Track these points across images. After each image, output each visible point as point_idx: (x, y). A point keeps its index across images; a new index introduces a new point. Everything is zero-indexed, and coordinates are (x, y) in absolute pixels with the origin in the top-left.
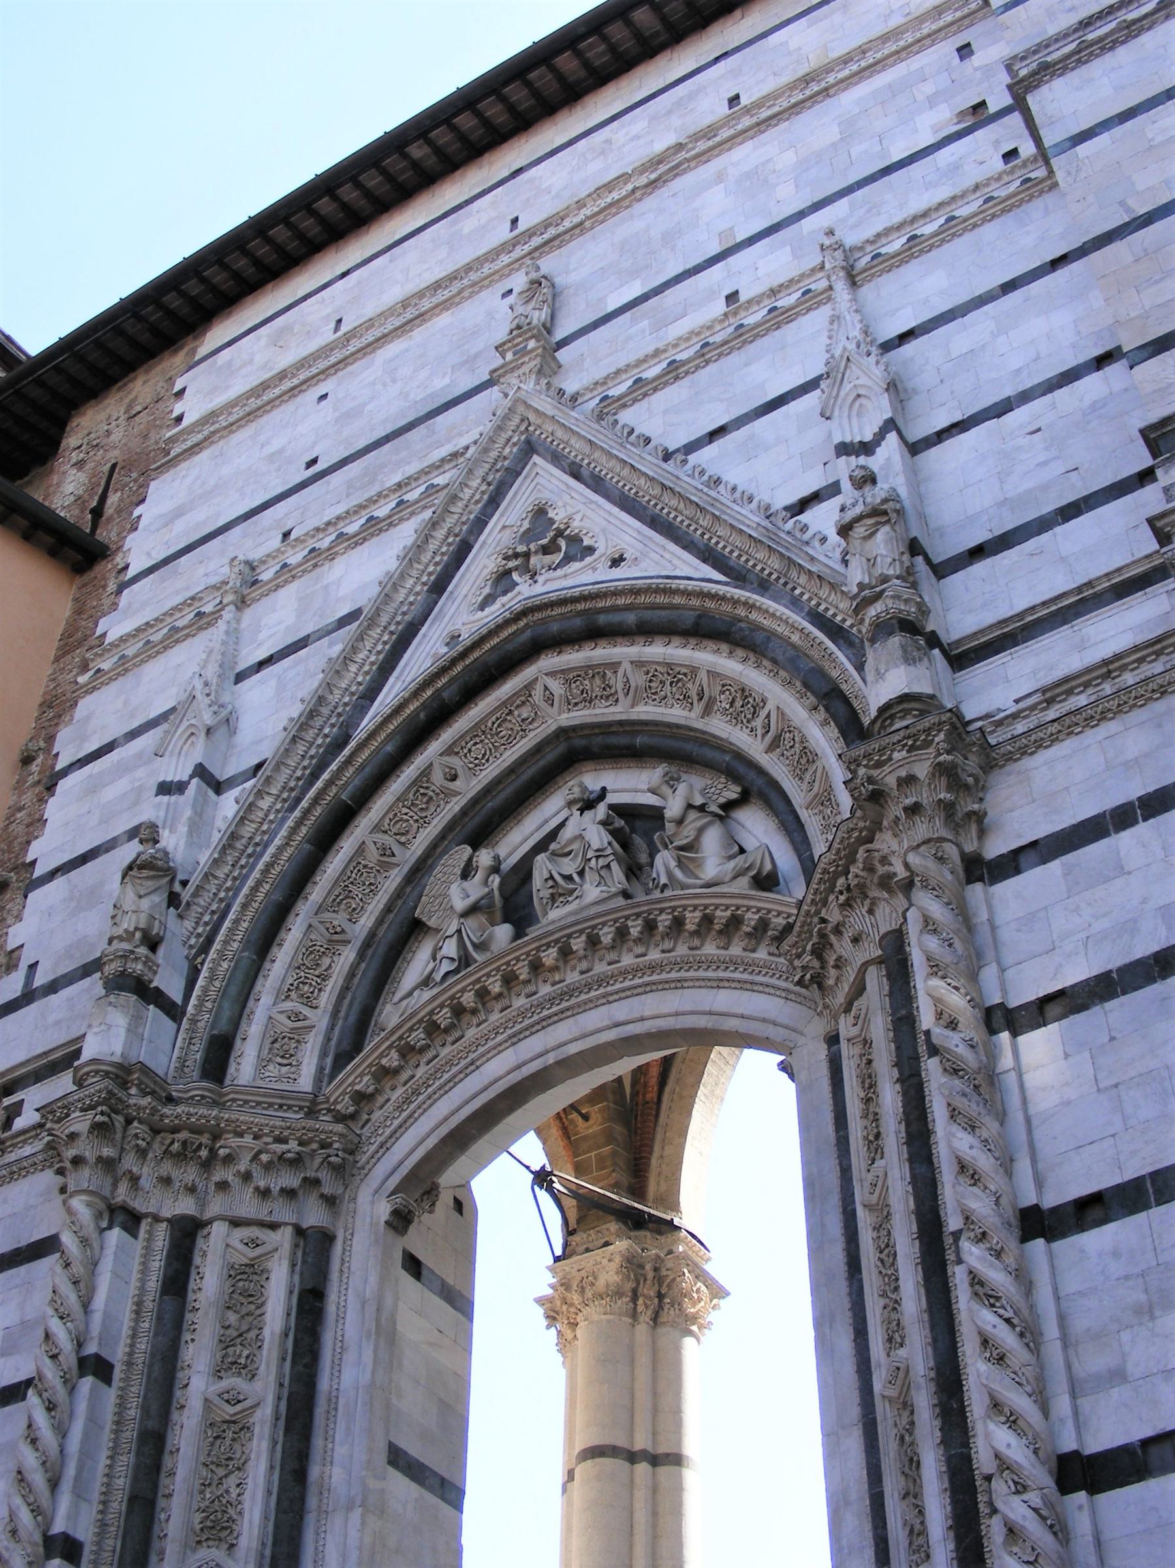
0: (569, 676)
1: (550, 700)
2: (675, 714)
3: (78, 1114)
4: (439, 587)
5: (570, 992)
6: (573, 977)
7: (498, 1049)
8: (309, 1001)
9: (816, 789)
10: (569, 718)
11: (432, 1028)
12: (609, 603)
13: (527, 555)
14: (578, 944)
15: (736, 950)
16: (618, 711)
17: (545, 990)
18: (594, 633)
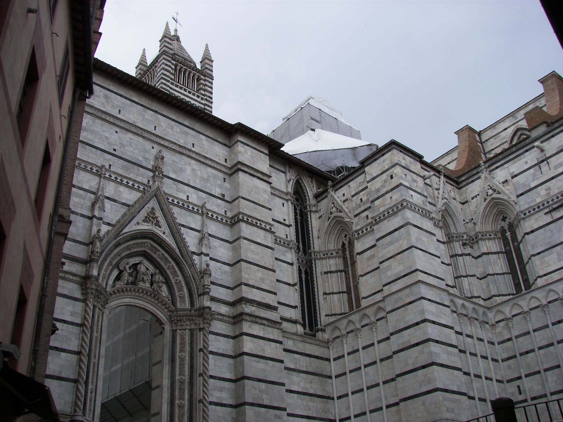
0: (151, 245)
1: (147, 246)
2: (163, 264)
3: (94, 285)
4: (139, 212)
5: (140, 297)
6: (141, 295)
7: (128, 298)
8: (106, 272)
9: (182, 296)
10: (147, 250)
11: (122, 290)
12: (164, 243)
13: (150, 216)
14: (145, 292)
15: (163, 307)
16: (155, 256)
17: (137, 294)
18: (160, 245)
